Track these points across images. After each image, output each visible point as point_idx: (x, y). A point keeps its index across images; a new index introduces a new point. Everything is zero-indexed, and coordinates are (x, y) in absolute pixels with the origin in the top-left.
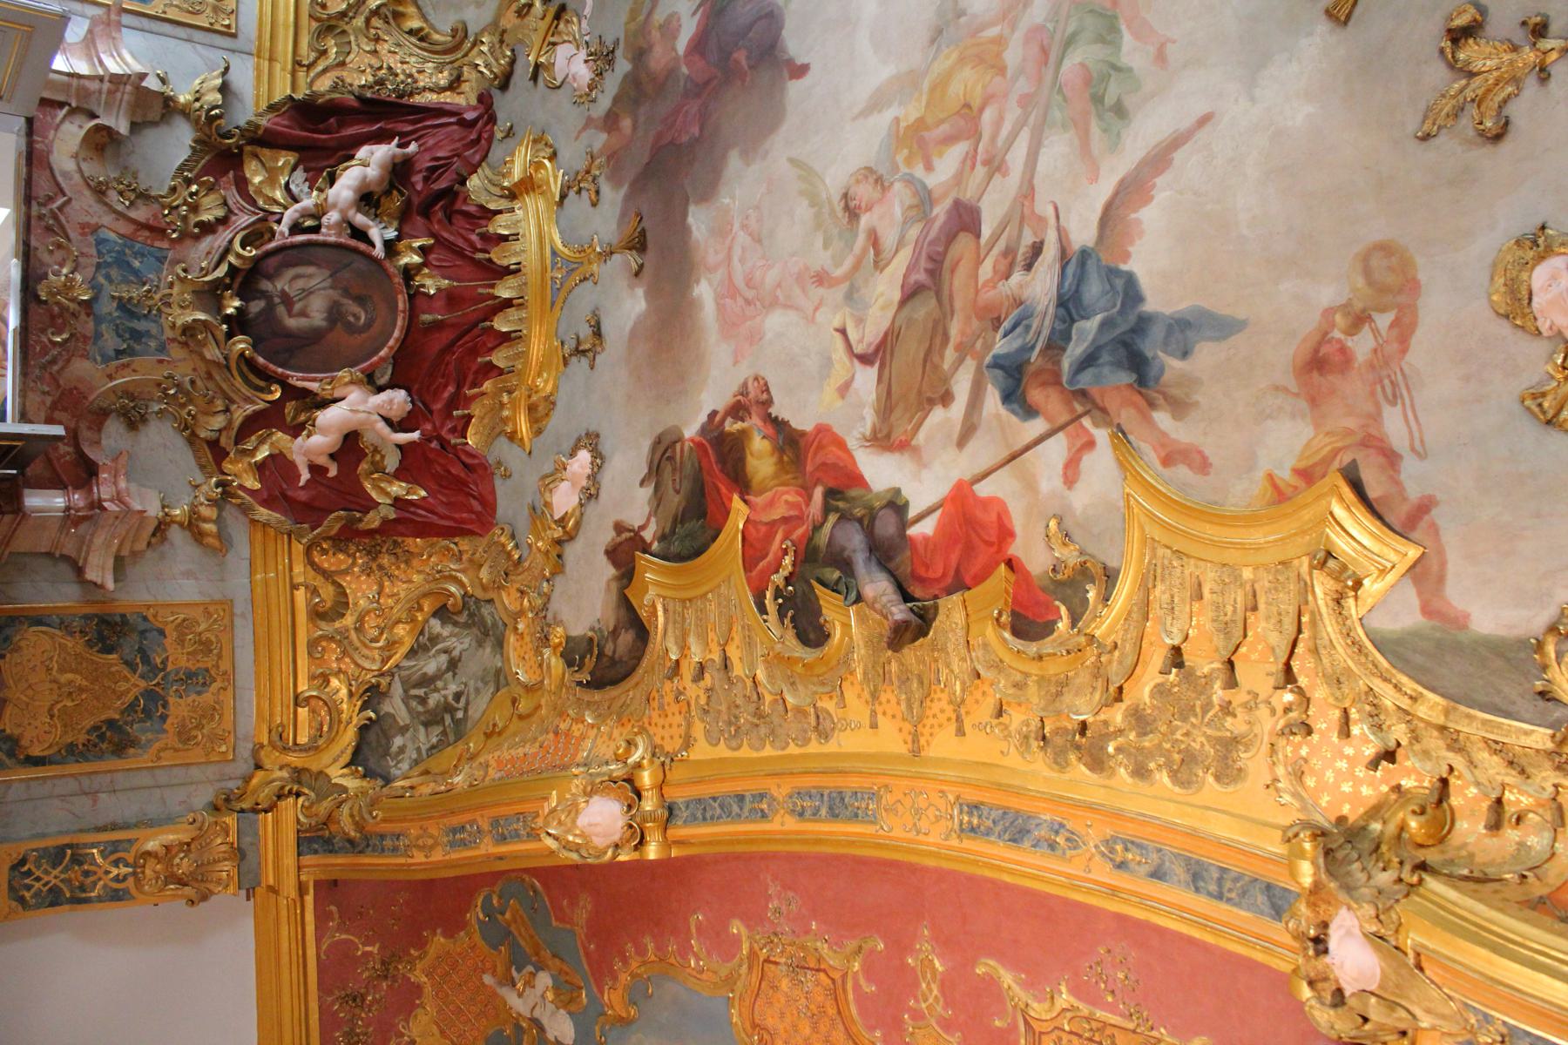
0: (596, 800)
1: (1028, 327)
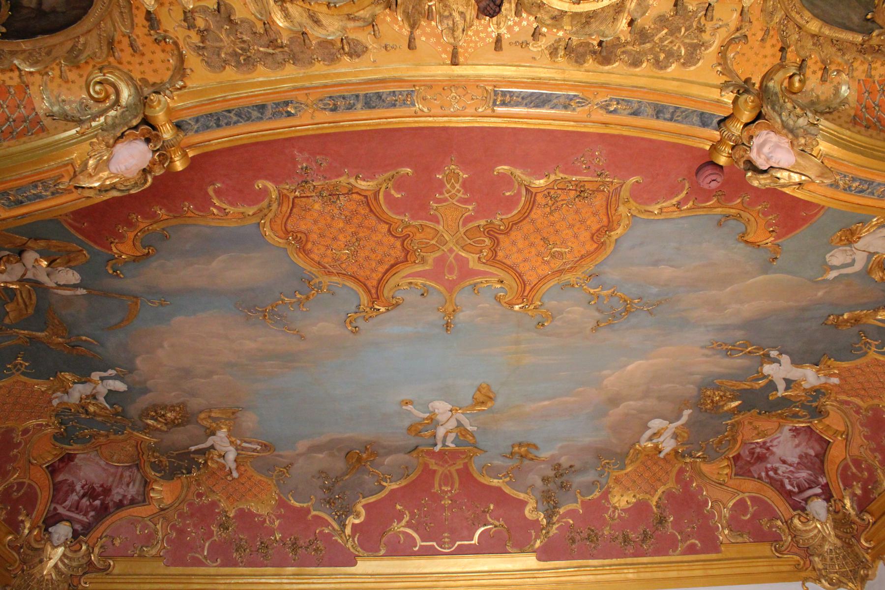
0: (119, 146)
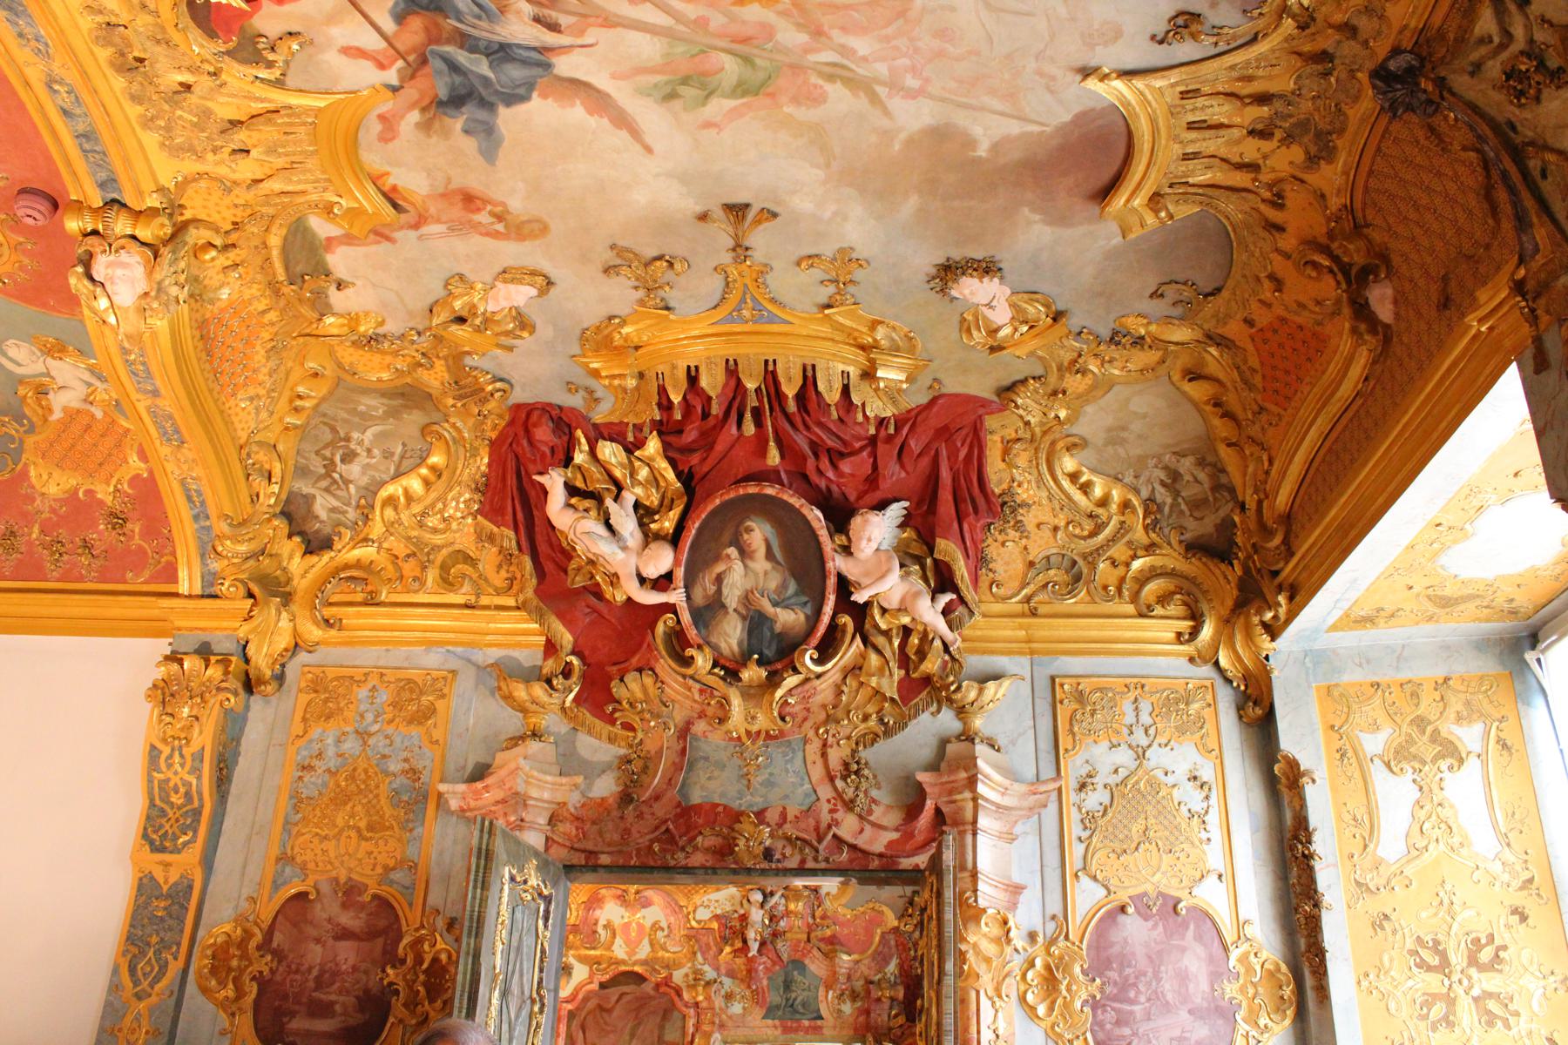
1: (479, 18)
